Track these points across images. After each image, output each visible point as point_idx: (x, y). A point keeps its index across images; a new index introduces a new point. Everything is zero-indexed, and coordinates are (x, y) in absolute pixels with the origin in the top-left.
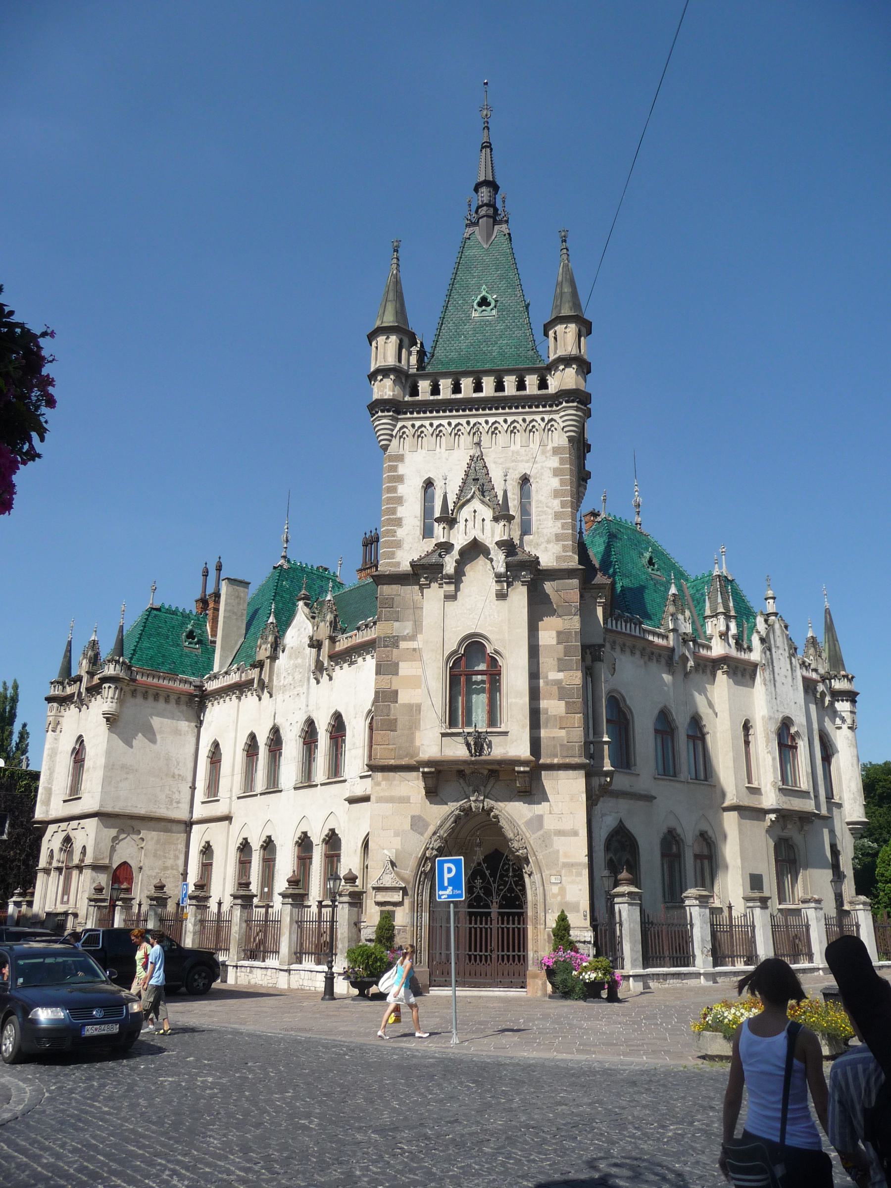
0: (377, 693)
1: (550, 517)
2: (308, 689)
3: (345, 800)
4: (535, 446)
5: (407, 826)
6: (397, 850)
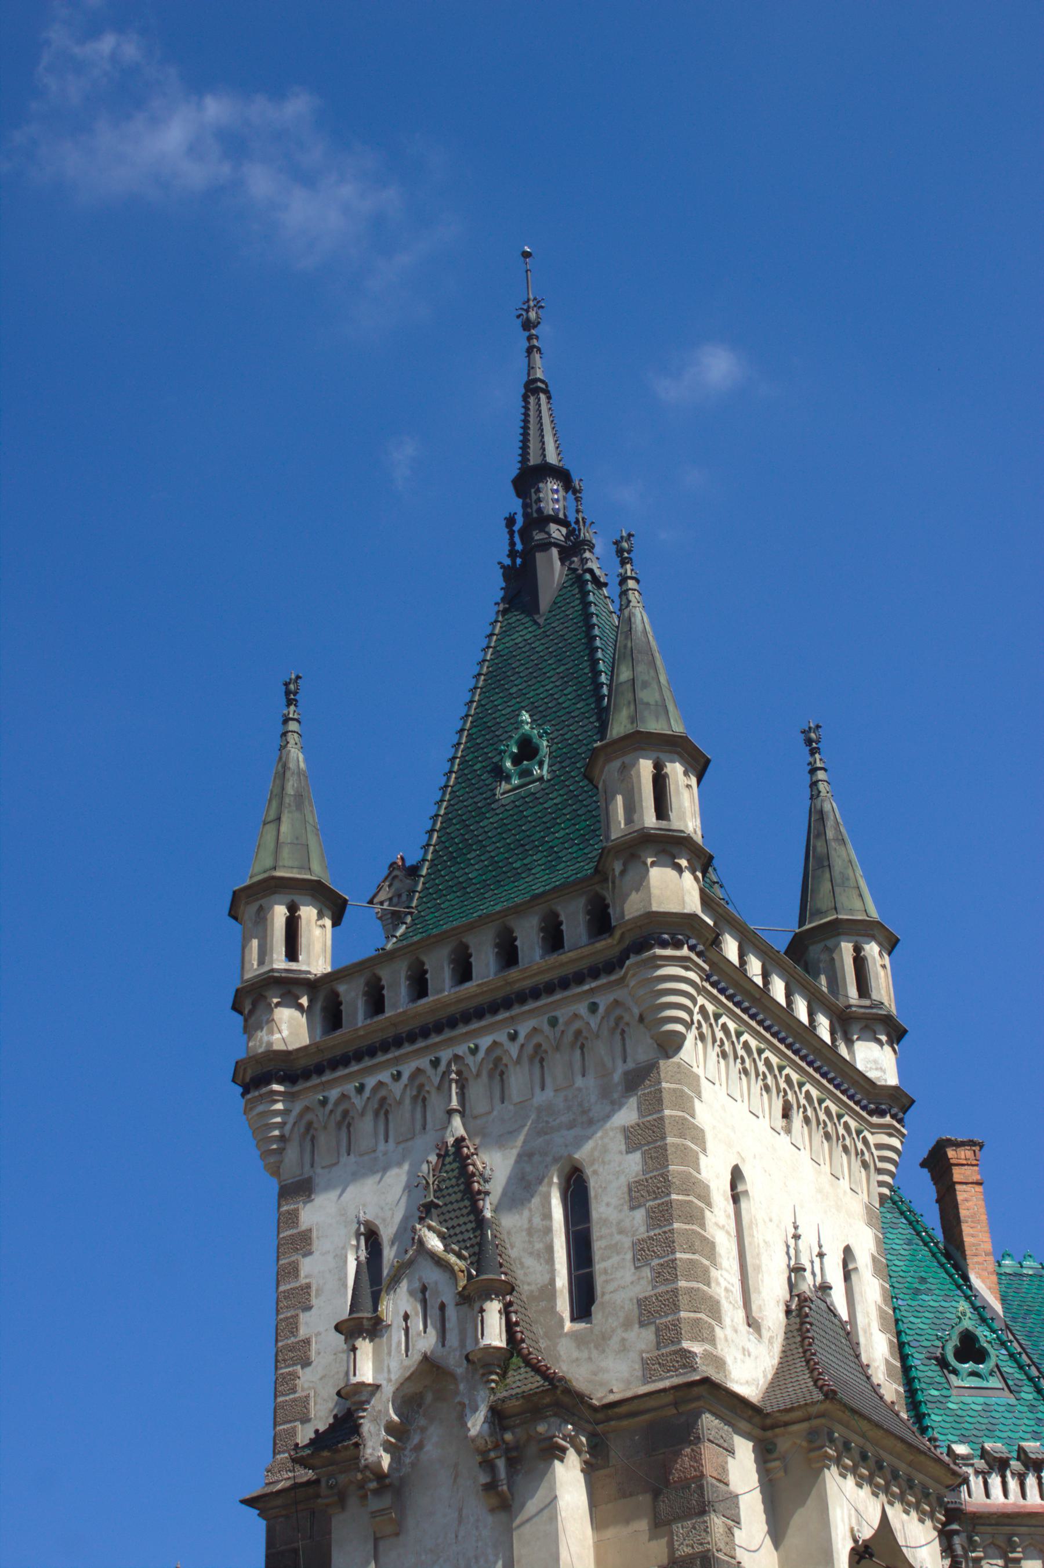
1: (629, 1256)
4: (587, 1084)
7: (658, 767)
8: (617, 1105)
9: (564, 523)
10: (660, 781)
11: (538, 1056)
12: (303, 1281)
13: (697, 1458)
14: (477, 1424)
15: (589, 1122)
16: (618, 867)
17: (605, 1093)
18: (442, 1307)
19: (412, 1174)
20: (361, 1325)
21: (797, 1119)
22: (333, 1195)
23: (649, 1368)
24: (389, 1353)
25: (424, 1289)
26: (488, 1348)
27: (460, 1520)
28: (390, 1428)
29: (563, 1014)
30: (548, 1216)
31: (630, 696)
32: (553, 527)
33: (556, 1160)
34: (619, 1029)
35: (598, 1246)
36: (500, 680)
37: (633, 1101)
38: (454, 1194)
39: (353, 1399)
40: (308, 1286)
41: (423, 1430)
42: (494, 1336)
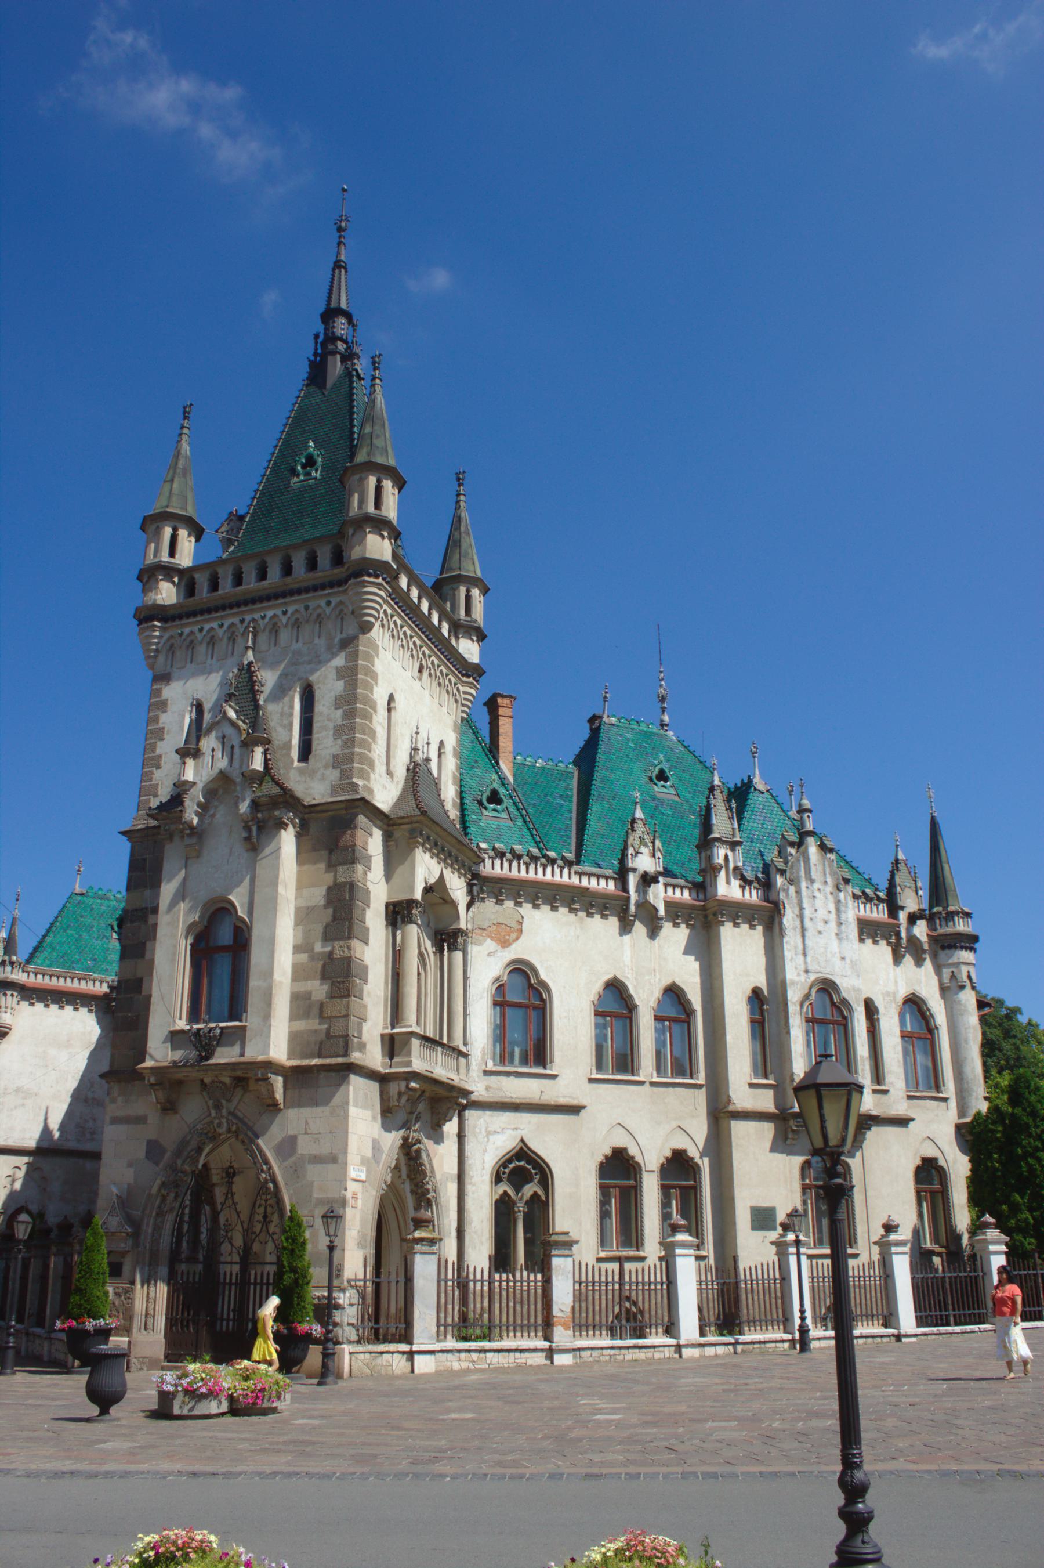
1: (331, 733)
4: (321, 643)
5: (142, 1154)
6: (129, 1185)
7: (379, 481)
8: (334, 655)
9: (345, 342)
10: (379, 489)
11: (297, 625)
12: (161, 725)
13: (353, 836)
14: (244, 807)
15: (318, 661)
16: (351, 531)
18: (232, 747)
19: (224, 677)
20: (189, 752)
21: (426, 673)
22: (181, 683)
23: (334, 790)
25: (224, 737)
26: (254, 770)
27: (231, 854)
28: (199, 805)
29: (312, 604)
30: (292, 707)
31: (369, 441)
32: (339, 343)
33: (299, 679)
34: (341, 616)
35: (316, 726)
36: (300, 422)
37: (343, 654)
38: (245, 690)
39: (181, 789)
40: (163, 728)
41: (216, 807)
42: (258, 764)
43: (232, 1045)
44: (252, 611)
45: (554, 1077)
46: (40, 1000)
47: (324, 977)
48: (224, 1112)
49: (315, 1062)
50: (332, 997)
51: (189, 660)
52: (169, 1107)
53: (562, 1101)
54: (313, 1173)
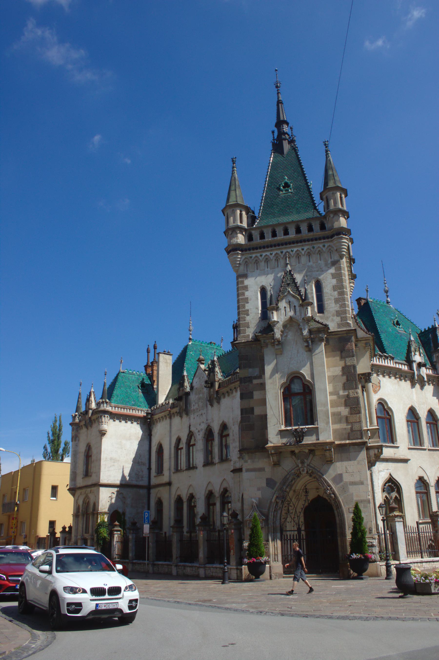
0: (242, 410)
1: (333, 301)
2: (207, 411)
3: (231, 471)
4: (322, 263)
5: (264, 484)
8: (330, 268)
9: (289, 135)
11: (309, 255)
14: (305, 332)
15: (323, 271)
16: (332, 216)
17: (326, 265)
18: (295, 306)
22: (253, 278)
23: (339, 325)
24: (281, 315)
25: (290, 302)
26: (309, 316)
27: (298, 352)
29: (316, 246)
30: (312, 290)
31: (333, 178)
32: (286, 135)
33: (314, 278)
34: (330, 252)
37: (333, 268)
40: (248, 298)
41: (287, 333)
43: (312, 435)
44: (285, 248)
45: (398, 447)
46: (118, 419)
47: (346, 405)
48: (306, 465)
49: (347, 442)
50: (351, 414)
51: (256, 268)
52: (277, 464)
53: (402, 457)
54: (352, 489)
